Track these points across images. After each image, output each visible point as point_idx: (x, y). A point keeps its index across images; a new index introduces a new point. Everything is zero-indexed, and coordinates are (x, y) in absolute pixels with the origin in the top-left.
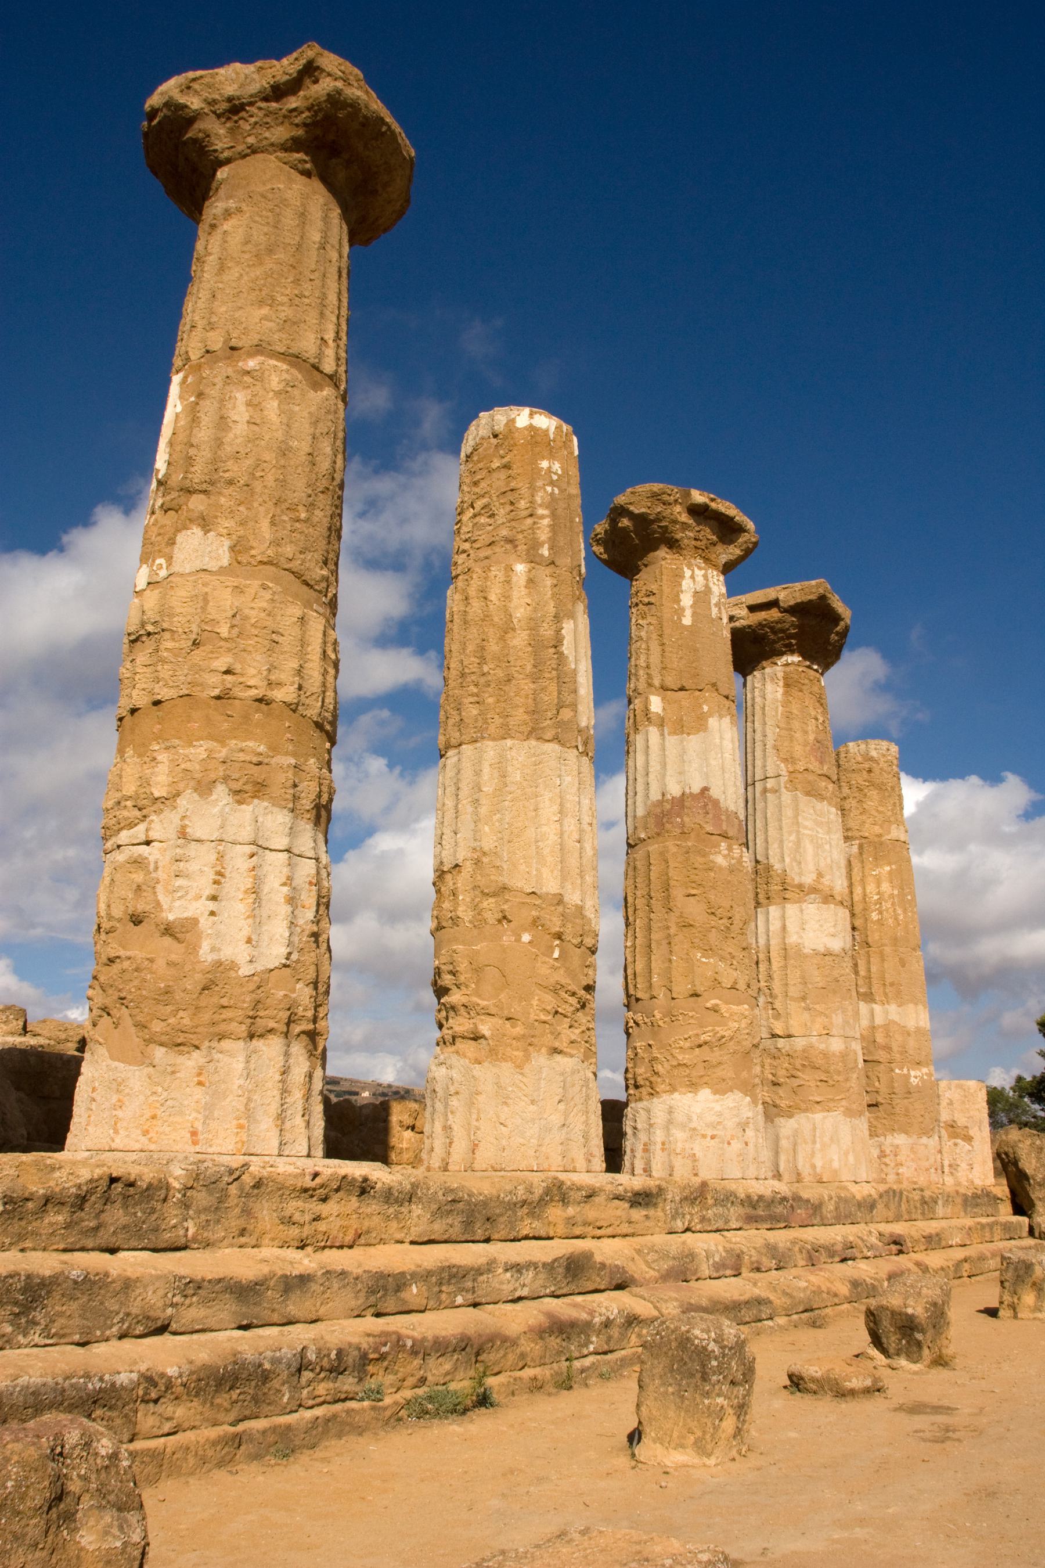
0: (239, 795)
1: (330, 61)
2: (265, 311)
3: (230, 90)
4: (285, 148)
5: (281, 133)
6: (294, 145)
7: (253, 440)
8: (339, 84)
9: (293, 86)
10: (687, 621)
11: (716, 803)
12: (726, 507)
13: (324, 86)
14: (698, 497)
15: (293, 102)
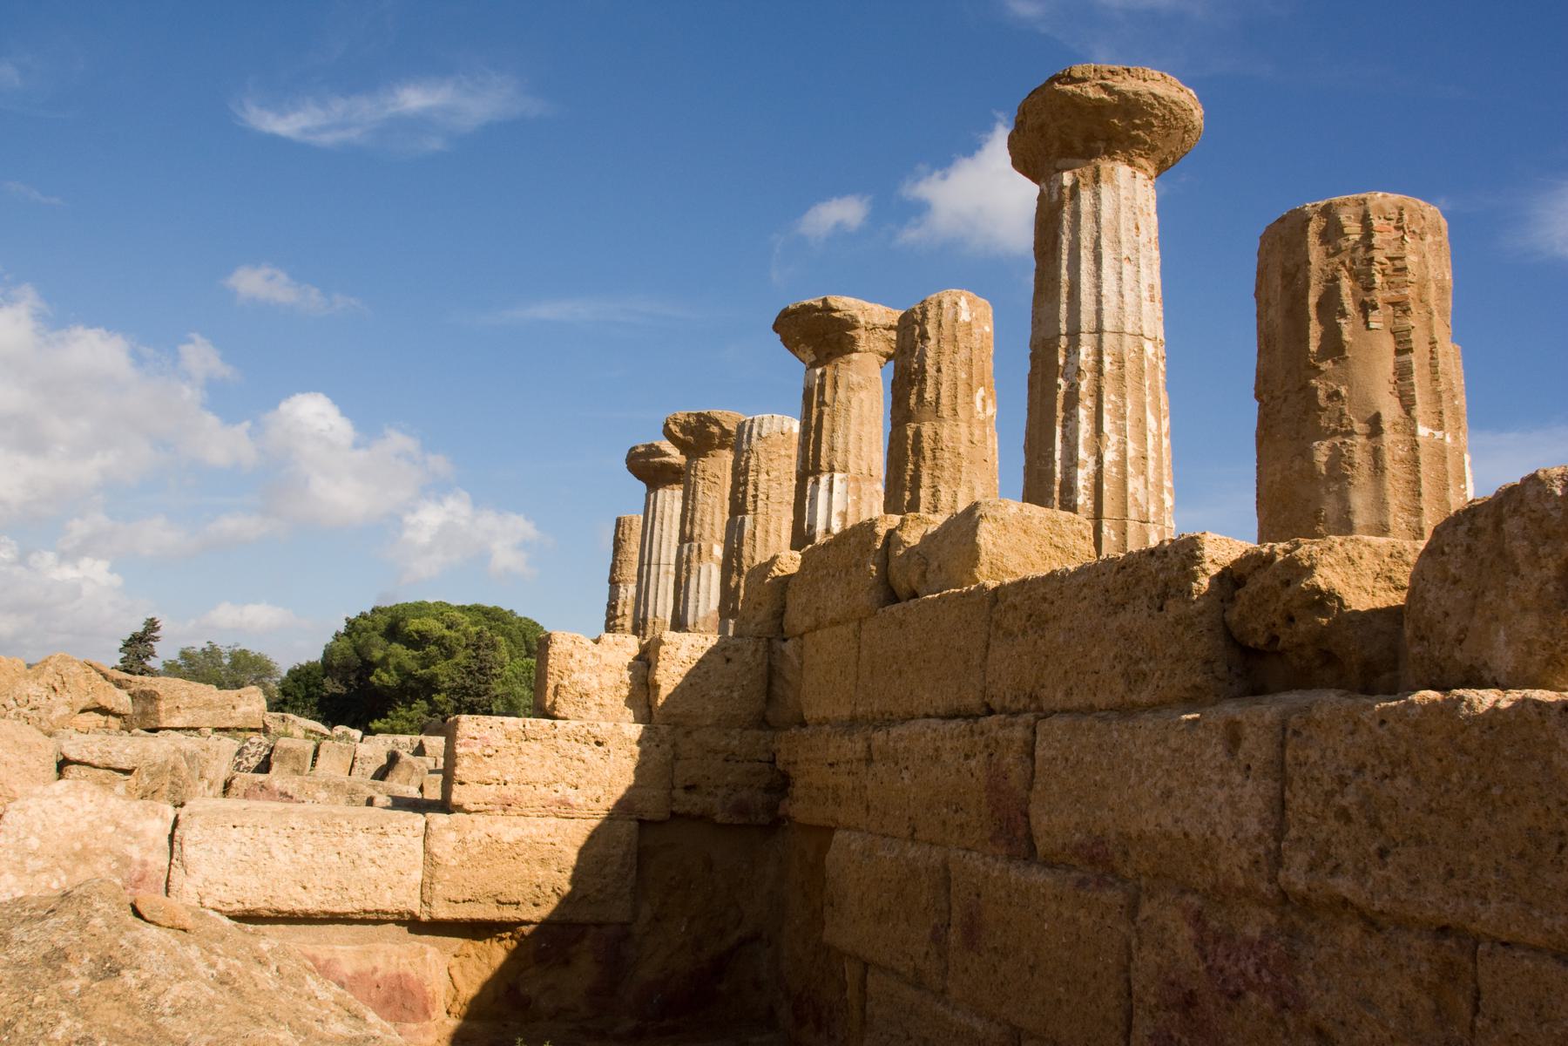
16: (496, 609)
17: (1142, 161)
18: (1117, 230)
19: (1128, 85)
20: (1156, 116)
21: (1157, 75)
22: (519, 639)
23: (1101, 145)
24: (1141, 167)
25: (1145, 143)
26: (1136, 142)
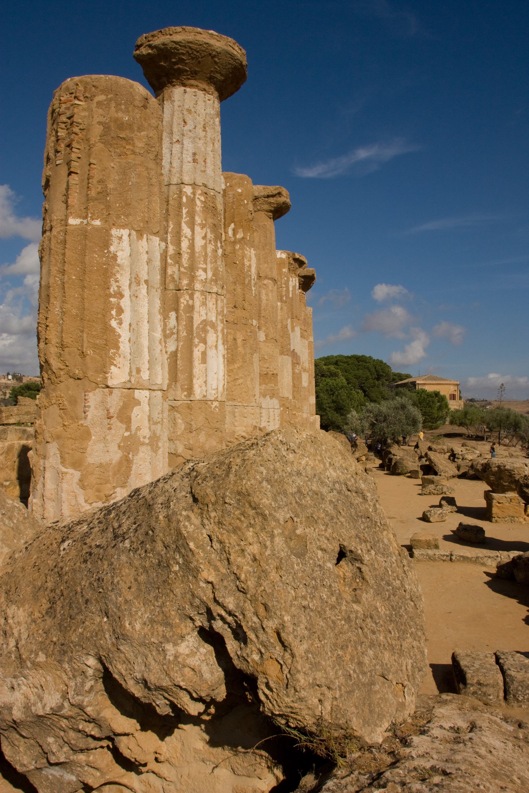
0: (271, 398)
1: (285, 192)
2: (266, 265)
3: (256, 194)
4: (267, 211)
5: (266, 207)
6: (271, 211)
7: (267, 305)
8: (285, 199)
9: (273, 196)
10: (291, 296)
11: (296, 353)
12: (303, 258)
13: (281, 200)
14: (297, 256)
15: (272, 200)
16: (363, 356)
17: (192, 82)
18: (171, 126)
19: (160, 40)
20: (183, 54)
21: (179, 29)
22: (373, 370)
23: (164, 79)
24: (191, 86)
25: (187, 71)
26: (180, 72)
